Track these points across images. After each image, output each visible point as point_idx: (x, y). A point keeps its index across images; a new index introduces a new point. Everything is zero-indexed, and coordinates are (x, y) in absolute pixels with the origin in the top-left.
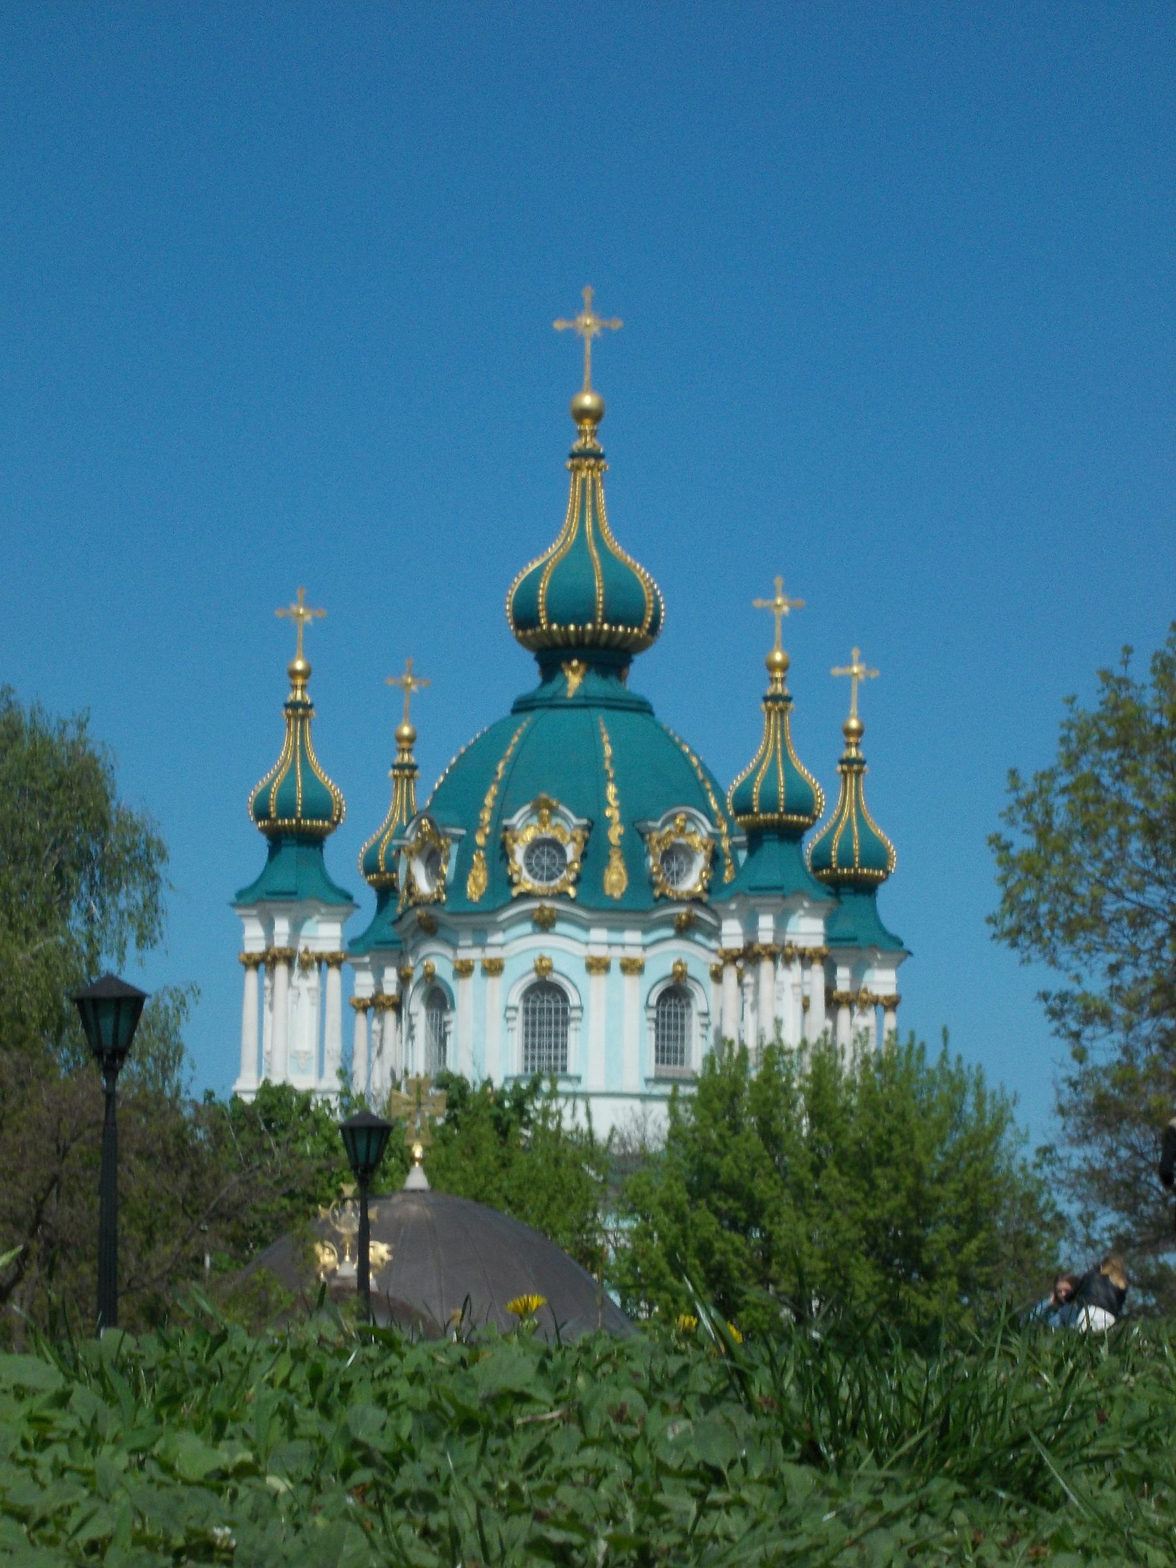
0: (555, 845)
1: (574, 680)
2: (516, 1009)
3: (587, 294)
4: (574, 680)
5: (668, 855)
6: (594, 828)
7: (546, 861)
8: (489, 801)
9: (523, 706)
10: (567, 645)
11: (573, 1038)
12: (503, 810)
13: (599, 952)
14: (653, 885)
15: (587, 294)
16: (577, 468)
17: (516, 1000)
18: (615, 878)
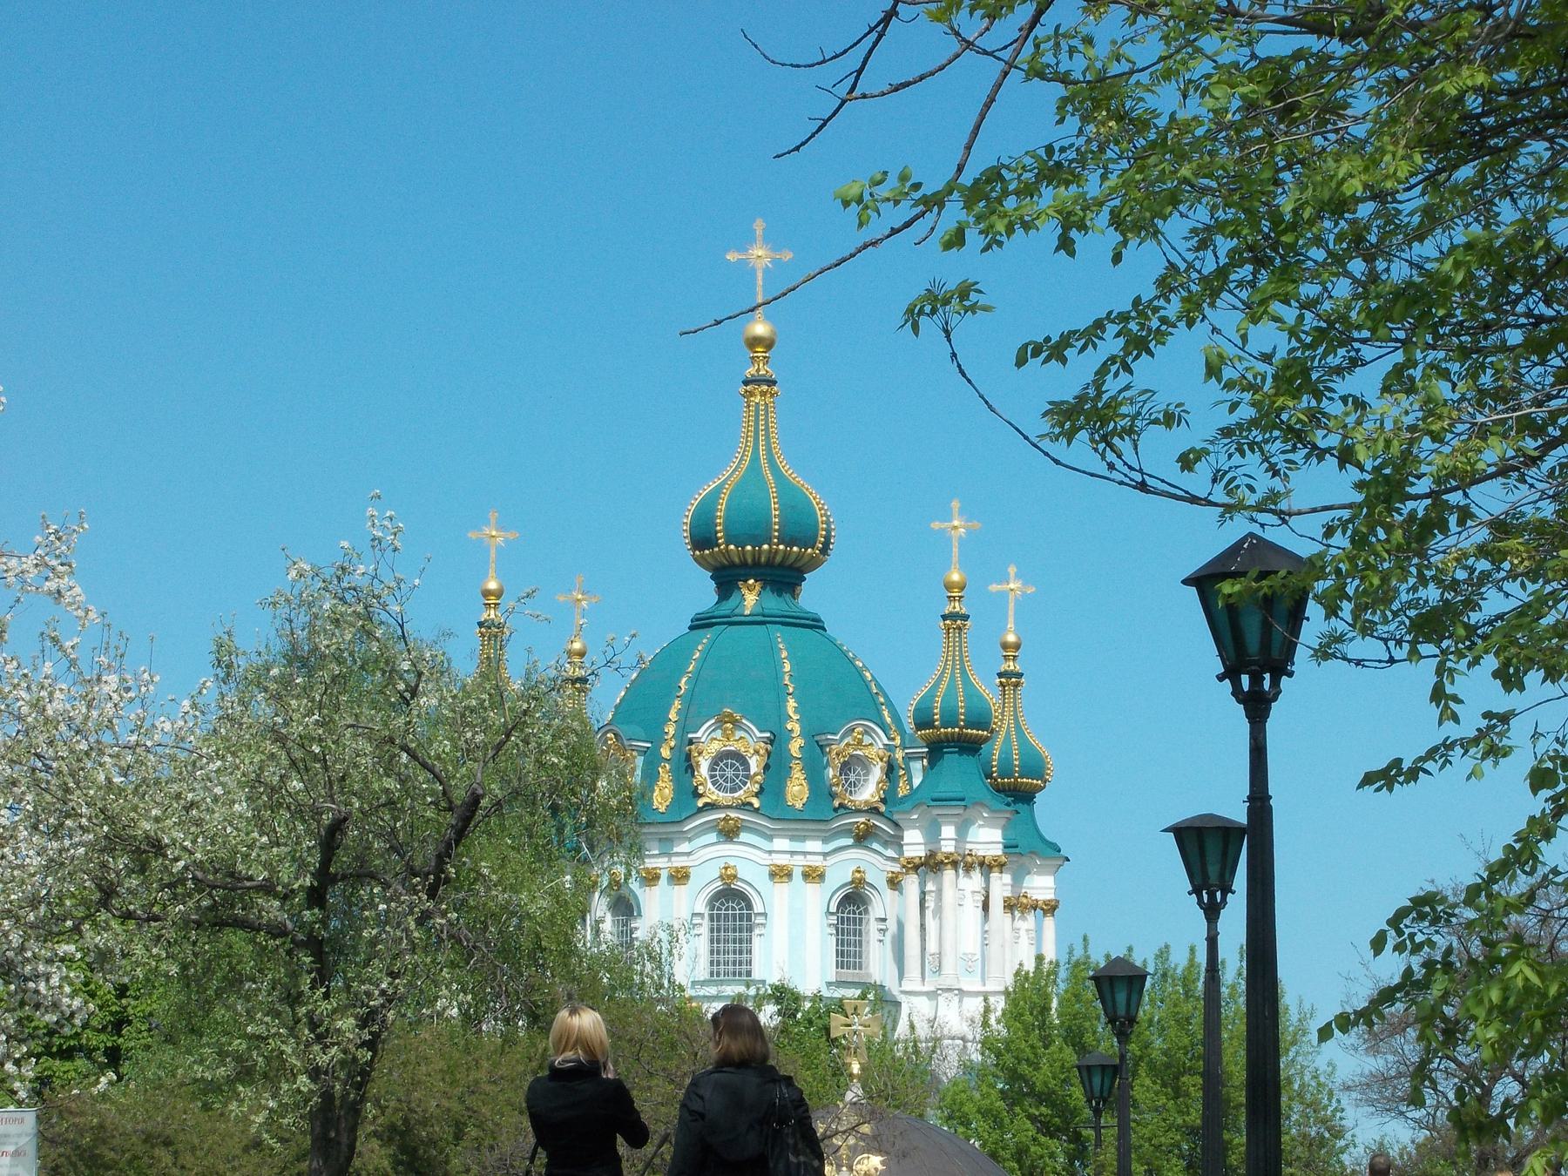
0: (740, 758)
1: (750, 598)
2: (701, 915)
3: (759, 226)
4: (750, 598)
5: (846, 767)
6: (776, 741)
7: (729, 773)
8: (673, 715)
9: (701, 623)
10: (744, 564)
11: (757, 943)
12: (687, 724)
13: (782, 860)
14: (833, 796)
15: (759, 226)
16: (752, 394)
17: (701, 907)
18: (797, 790)
